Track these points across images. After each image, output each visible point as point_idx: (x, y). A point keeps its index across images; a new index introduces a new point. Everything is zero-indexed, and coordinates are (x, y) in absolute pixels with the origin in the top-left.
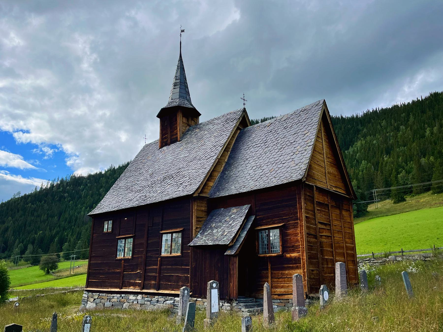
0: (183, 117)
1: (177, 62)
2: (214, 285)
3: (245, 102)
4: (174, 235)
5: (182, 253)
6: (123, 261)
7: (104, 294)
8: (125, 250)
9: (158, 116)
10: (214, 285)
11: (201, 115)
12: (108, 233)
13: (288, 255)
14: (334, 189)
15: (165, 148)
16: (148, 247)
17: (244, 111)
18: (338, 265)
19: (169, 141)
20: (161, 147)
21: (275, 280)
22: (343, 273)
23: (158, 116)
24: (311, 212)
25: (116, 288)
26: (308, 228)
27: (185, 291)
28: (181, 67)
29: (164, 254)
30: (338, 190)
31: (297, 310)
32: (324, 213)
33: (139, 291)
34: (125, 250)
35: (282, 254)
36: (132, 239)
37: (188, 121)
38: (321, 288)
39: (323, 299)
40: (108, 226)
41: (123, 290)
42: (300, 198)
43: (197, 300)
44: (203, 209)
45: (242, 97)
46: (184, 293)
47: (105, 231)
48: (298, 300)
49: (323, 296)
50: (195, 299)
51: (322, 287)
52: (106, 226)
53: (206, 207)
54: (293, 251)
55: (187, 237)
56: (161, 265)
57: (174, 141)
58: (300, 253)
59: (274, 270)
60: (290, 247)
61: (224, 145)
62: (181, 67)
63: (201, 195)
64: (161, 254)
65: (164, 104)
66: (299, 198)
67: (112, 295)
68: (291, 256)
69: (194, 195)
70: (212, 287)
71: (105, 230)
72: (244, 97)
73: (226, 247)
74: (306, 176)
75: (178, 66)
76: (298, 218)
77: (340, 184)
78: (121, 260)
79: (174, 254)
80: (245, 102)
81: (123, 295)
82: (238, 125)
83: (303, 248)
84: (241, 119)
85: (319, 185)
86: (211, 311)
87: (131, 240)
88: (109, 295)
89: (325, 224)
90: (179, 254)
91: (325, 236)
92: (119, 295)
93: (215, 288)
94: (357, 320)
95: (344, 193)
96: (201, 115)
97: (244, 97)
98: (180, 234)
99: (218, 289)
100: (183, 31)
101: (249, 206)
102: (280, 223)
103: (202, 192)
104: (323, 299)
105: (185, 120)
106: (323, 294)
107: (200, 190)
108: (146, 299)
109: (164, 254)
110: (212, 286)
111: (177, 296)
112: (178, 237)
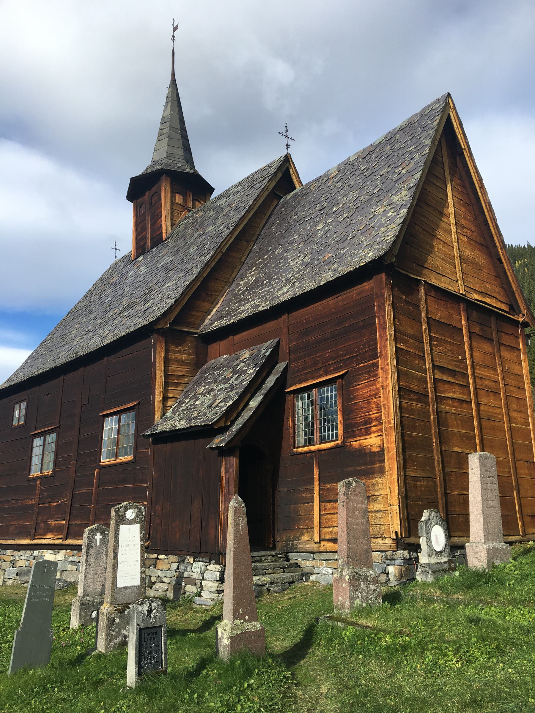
0: (173, 193)
1: (165, 90)
2: (130, 514)
3: (290, 142)
4: (123, 416)
5: (135, 456)
6: (39, 482)
7: (9, 552)
8: (42, 459)
9: (130, 197)
10: (130, 514)
11: (213, 189)
12: (19, 427)
13: (356, 444)
14: (476, 296)
15: (141, 258)
16: (80, 446)
17: (287, 160)
18: (474, 461)
19: (149, 242)
20: (137, 257)
21: (329, 505)
22: (489, 480)
24: (412, 341)
25: (26, 536)
26: (399, 374)
27: (93, 535)
28: (174, 99)
29: (104, 461)
30: (488, 300)
31: (347, 578)
32: (449, 347)
33: (60, 542)
34: (42, 459)
35: (343, 442)
37: (185, 200)
38: (423, 519)
39: (429, 546)
40: (19, 413)
41: (36, 542)
42: (382, 307)
43: (157, 558)
44: (184, 357)
45: (283, 131)
46: (91, 539)
47: (14, 423)
48: (349, 549)
49: (429, 540)
50: (156, 555)
51: (426, 514)
52: (17, 416)
53: (190, 354)
54: (368, 432)
55: (144, 418)
56: (99, 484)
57: (158, 240)
58: (381, 439)
59: (325, 483)
60: (360, 424)
61: (237, 225)
62: (174, 99)
63: (178, 328)
64: (100, 462)
65: (138, 170)
66: (379, 306)
67: (21, 553)
68: (360, 445)
69: (159, 327)
70: (122, 520)
71: (15, 423)
72: (287, 131)
73: (208, 431)
74: (396, 253)
75: (167, 98)
76: (377, 353)
77: (493, 287)
78: (37, 478)
79: (122, 459)
80: (290, 142)
81: (36, 553)
82: (271, 187)
83: (389, 423)
84: (280, 175)
85: (433, 281)
86: (114, 583)
87: (52, 438)
88: (16, 553)
89: (452, 373)
90: (130, 458)
91: (452, 399)
92: (29, 553)
93: (131, 522)
94: (436, 627)
95: (504, 307)
96: (213, 189)
97: (287, 131)
98: (132, 414)
100: (175, 29)
101: (277, 339)
102: (337, 370)
103: (177, 321)
104: (429, 546)
105: (178, 199)
106: (428, 535)
107: (172, 317)
108: (71, 559)
109: (104, 461)
110: (124, 516)
111: (78, 548)
112: (129, 421)
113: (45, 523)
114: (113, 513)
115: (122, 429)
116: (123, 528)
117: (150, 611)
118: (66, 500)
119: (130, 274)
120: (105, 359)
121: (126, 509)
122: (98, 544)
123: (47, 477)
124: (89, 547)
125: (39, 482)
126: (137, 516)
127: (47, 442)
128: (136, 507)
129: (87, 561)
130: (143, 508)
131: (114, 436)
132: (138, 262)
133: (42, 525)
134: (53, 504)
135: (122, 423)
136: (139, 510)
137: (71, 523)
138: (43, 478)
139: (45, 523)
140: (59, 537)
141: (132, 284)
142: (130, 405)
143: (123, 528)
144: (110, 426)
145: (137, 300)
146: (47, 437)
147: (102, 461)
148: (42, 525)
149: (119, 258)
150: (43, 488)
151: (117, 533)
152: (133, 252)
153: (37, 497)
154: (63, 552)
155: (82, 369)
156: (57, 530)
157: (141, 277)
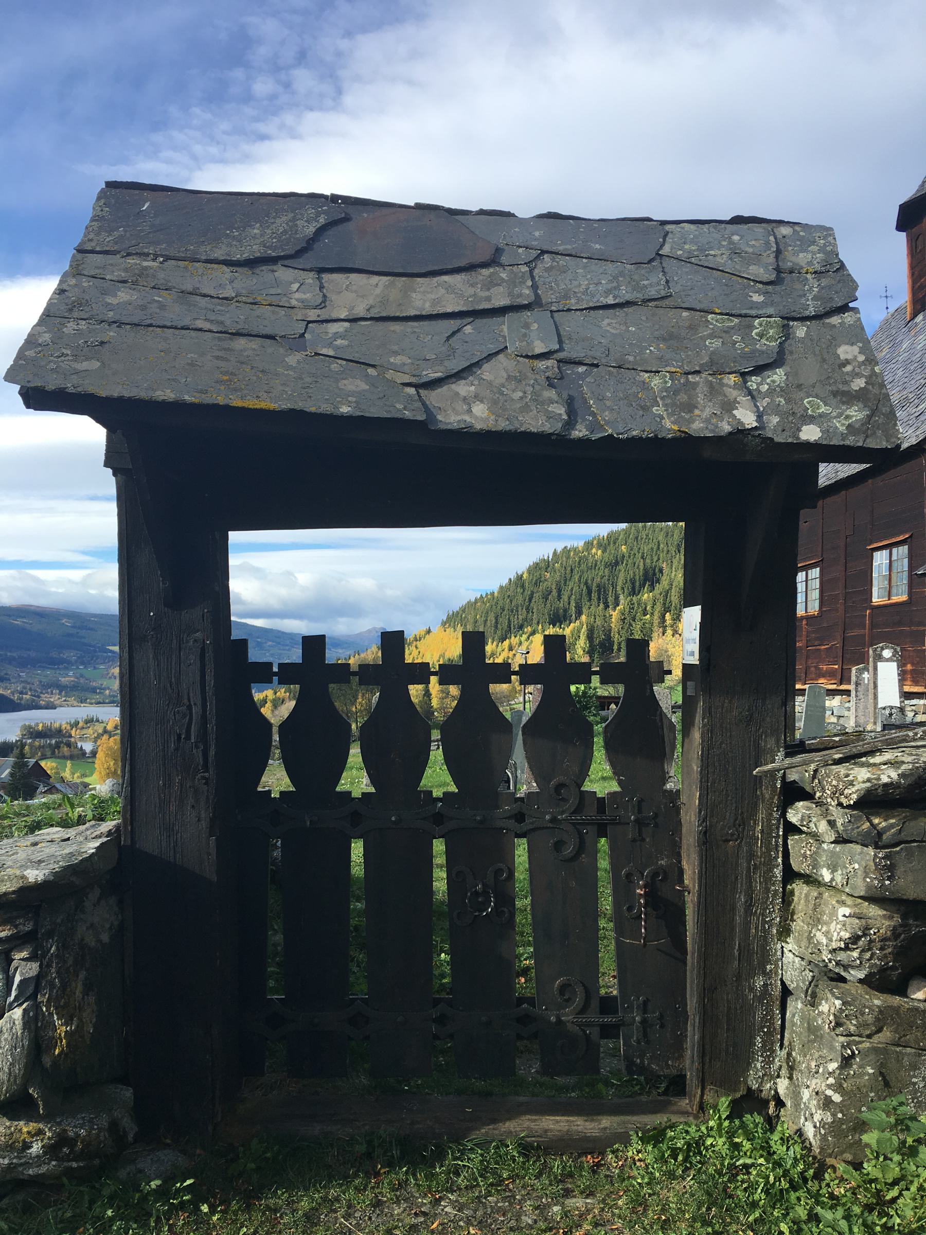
4: (895, 550)
5: (910, 594)
6: (804, 622)
10: (887, 653)
15: (920, 317)
23: (900, 228)
33: (834, 687)
36: (818, 569)
56: (873, 626)
70: (879, 658)
79: (895, 599)
90: (904, 598)
93: (888, 660)
99: (897, 661)
113: (815, 667)
114: (871, 652)
115: (895, 565)
116: (880, 665)
117: (891, 715)
118: (837, 643)
119: (904, 347)
120: (870, 481)
121: (882, 649)
122: (866, 682)
123: (813, 617)
124: (857, 684)
125: (804, 622)
126: (894, 656)
127: (809, 578)
128: (892, 648)
129: (856, 696)
130: (899, 649)
131: (885, 572)
132: (916, 324)
133: (813, 669)
134: (823, 647)
135: (894, 557)
136: (895, 650)
137: (845, 667)
138: (809, 618)
139: (815, 667)
140: (833, 682)
141: (907, 363)
142: (902, 538)
143: (880, 665)
144: (880, 559)
145: (911, 396)
146: (810, 571)
147: (874, 600)
148: (813, 669)
149: (892, 310)
150: (810, 629)
151: (875, 669)
152: (908, 304)
153: (804, 638)
154: (838, 698)
155: (844, 492)
156: (830, 675)
157: (918, 355)
